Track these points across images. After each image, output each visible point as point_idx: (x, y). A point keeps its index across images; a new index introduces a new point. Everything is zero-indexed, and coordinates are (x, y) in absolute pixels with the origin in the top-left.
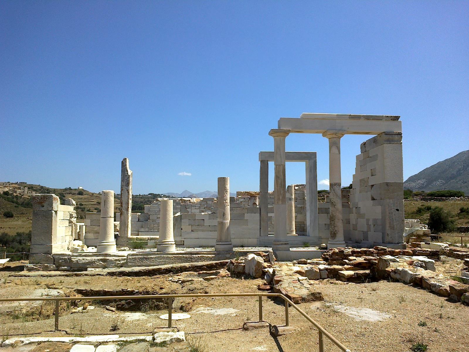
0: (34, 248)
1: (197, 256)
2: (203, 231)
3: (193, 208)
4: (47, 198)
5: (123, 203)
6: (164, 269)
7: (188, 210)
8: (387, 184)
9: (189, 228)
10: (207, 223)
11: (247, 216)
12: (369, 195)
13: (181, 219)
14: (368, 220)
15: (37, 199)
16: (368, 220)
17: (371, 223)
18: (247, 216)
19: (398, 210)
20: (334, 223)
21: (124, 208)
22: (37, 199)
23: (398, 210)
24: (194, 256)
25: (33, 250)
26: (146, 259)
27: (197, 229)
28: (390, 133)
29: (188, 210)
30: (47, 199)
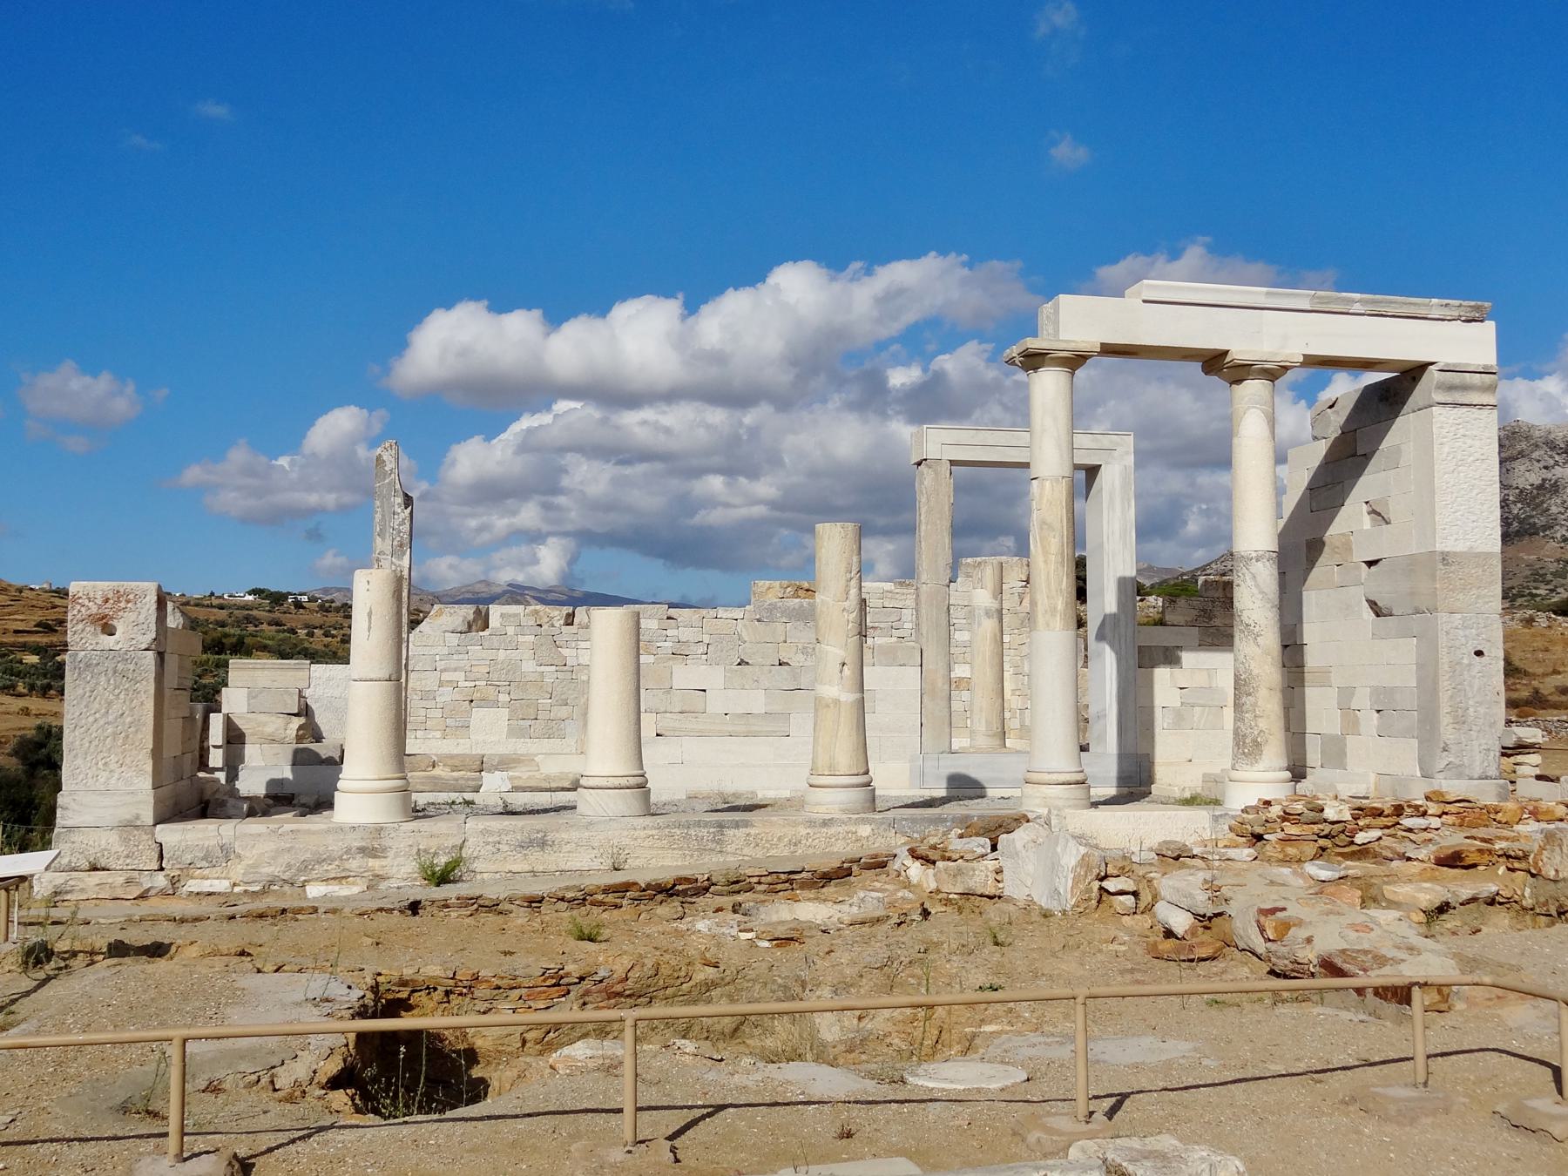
0: (73, 805)
2: (701, 734)
6: (649, 887)
7: (565, 652)
8: (1445, 558)
12: (1358, 596)
14: (1347, 693)
16: (1347, 693)
17: (1363, 700)
19: (1479, 653)
20: (1255, 705)
23: (1479, 653)
25: (69, 813)
26: (543, 844)
27: (677, 725)
29: (565, 652)
30: (128, 601)
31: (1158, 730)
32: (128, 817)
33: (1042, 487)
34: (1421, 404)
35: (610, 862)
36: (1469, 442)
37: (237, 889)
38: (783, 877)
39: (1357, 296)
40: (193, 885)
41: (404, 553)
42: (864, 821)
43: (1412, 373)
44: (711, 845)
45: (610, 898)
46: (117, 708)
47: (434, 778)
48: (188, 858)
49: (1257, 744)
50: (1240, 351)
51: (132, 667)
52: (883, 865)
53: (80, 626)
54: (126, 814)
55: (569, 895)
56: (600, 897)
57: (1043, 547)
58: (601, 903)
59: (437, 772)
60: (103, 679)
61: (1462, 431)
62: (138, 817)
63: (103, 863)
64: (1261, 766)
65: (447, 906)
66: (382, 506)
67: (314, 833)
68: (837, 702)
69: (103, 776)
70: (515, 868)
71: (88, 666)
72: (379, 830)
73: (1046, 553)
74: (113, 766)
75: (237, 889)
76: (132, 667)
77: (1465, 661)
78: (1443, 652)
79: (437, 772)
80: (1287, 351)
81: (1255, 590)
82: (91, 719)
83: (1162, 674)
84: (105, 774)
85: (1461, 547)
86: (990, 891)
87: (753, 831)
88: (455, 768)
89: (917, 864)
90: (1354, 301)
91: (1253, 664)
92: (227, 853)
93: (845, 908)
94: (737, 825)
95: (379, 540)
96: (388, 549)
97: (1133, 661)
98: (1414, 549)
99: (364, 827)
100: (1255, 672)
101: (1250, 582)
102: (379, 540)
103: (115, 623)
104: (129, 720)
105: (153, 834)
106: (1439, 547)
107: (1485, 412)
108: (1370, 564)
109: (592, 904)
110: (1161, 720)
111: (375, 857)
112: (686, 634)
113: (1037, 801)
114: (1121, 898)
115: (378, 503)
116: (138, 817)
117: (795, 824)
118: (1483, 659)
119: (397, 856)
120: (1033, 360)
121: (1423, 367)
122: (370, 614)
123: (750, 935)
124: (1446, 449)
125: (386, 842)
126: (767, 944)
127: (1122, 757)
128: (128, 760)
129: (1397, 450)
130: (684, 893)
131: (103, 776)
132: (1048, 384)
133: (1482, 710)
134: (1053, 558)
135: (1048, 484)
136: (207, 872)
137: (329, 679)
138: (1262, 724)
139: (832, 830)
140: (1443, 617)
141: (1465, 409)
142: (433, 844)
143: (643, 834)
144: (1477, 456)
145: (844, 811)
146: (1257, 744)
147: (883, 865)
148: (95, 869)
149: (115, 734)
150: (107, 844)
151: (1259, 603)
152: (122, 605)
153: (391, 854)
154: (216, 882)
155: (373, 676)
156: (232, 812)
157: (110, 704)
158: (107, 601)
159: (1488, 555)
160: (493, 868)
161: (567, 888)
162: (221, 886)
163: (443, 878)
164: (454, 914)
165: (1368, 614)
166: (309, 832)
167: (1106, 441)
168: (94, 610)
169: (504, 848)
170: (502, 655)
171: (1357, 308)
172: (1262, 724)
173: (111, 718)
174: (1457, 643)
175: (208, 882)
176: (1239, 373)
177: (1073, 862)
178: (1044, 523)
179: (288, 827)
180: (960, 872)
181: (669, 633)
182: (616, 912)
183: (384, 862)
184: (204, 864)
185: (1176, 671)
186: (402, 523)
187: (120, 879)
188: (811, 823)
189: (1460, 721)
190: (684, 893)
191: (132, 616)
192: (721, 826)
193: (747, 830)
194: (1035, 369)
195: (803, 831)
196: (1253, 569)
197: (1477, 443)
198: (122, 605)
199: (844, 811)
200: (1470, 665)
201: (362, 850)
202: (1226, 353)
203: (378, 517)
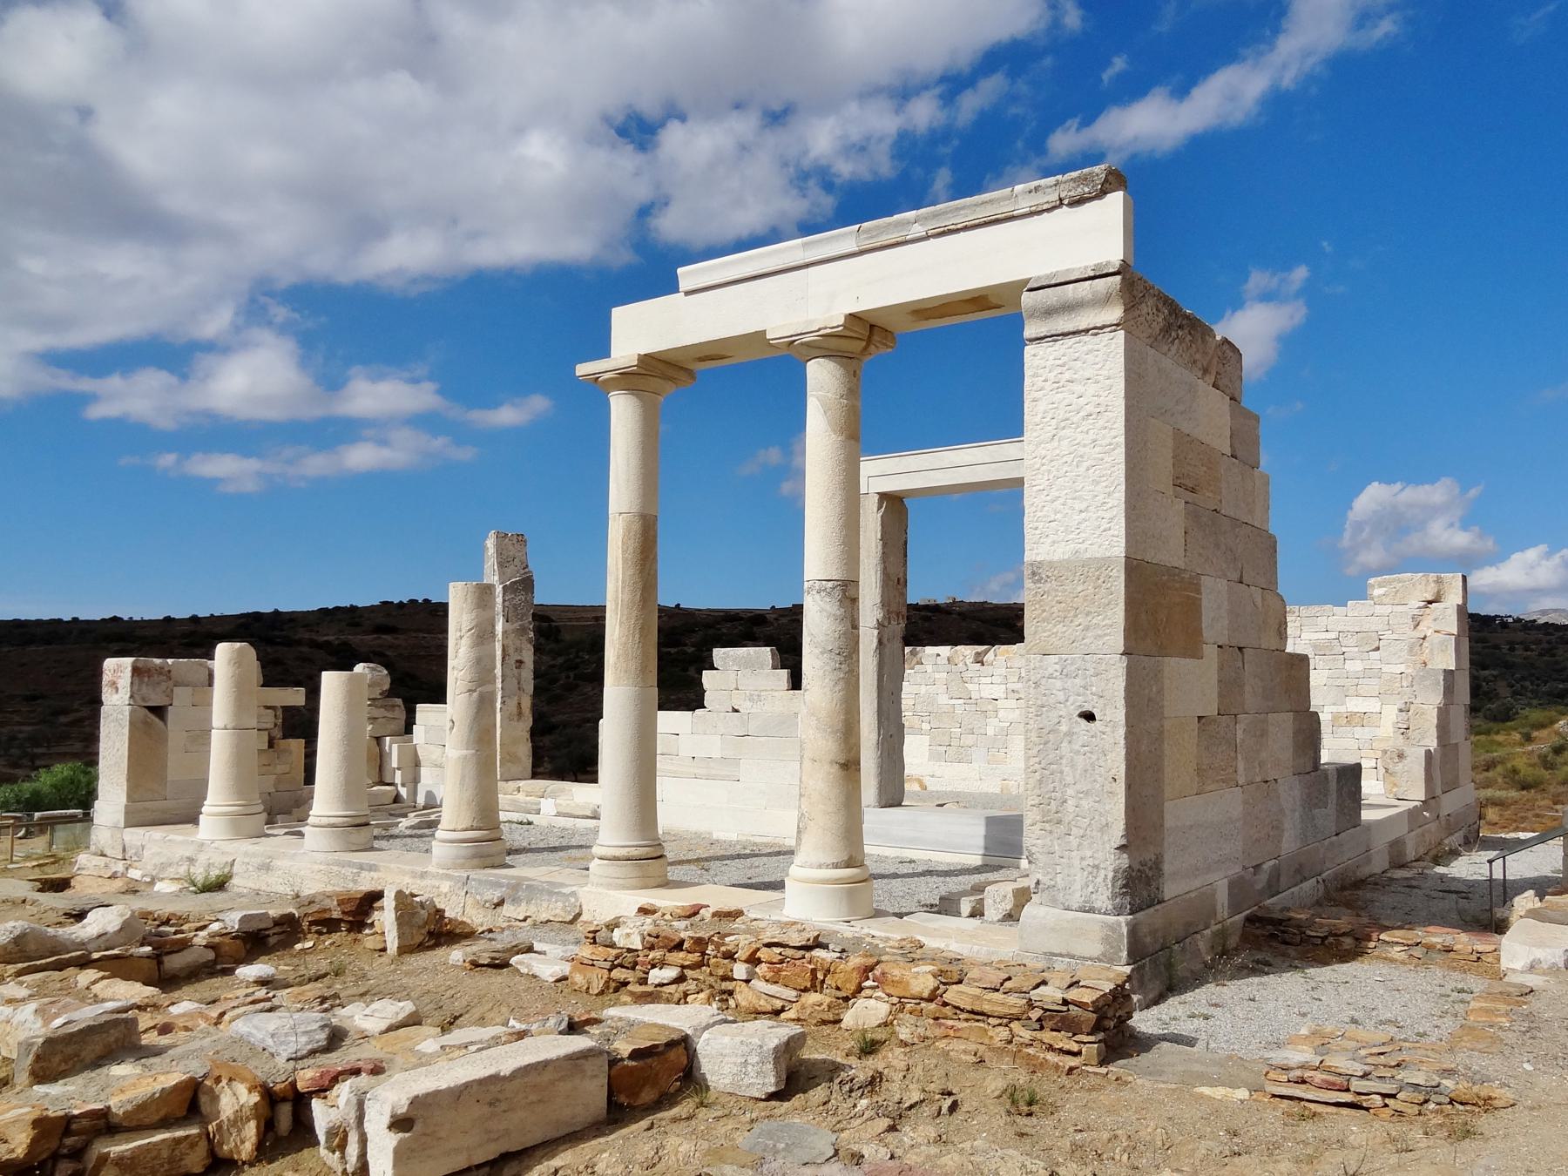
3: (983, 680)
7: (970, 686)
19: (1089, 717)
23: (1089, 717)
28: (1047, 277)
29: (970, 686)
36: (1078, 388)
61: (1067, 376)
77: (1064, 728)
85: (1061, 552)
107: (1105, 337)
118: (1092, 725)
133: (1086, 804)
144: (1090, 408)
159: (1105, 562)
170: (923, 689)
174: (1052, 700)
197: (1092, 389)
200: (1070, 734)
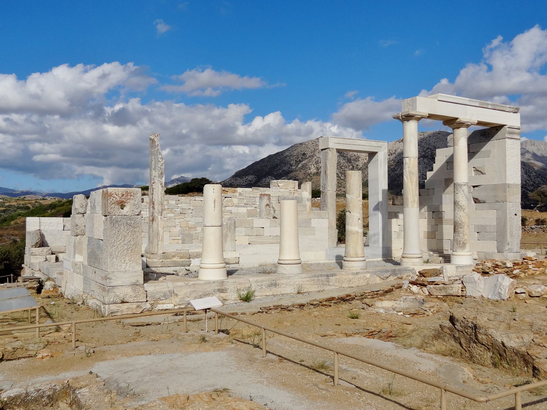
1: (334, 278)
2: (263, 243)
4: (132, 194)
5: (156, 203)
6: (339, 298)
8: (509, 184)
9: (246, 240)
10: (268, 232)
11: (315, 222)
13: (235, 227)
15: (115, 196)
18: (315, 222)
20: (464, 231)
21: (156, 210)
22: (115, 196)
23: (516, 215)
24: (331, 278)
25: (112, 281)
26: (275, 285)
27: (255, 240)
30: (131, 196)
31: (393, 239)
32: (134, 281)
33: (410, 161)
34: (500, 138)
35: (296, 290)
37: (176, 307)
38: (375, 293)
39: (490, 103)
40: (160, 307)
41: (163, 177)
42: (368, 272)
43: (498, 128)
44: (326, 283)
45: (327, 303)
46: (128, 238)
47: (174, 261)
48: (158, 296)
49: (464, 243)
50: (462, 118)
51: (133, 222)
52: (401, 287)
53: (113, 206)
54: (133, 280)
55: (315, 303)
56: (325, 303)
57: (411, 180)
58: (325, 305)
59: (174, 259)
60: (122, 227)
62: (138, 281)
63: (126, 300)
64: (466, 250)
65: (271, 309)
66: (155, 158)
67: (200, 284)
68: (357, 232)
69: (124, 266)
70: (268, 294)
71: (117, 221)
72: (222, 282)
73: (412, 182)
74: (126, 262)
75: (176, 307)
76: (133, 222)
78: (508, 214)
79: (174, 259)
80: (473, 119)
81: (463, 195)
82: (118, 243)
83: (394, 221)
84: (124, 265)
85: (512, 182)
86: (460, 294)
87: (337, 277)
88: (181, 258)
89: (415, 286)
90: (488, 104)
91: (463, 218)
92: (172, 293)
93: (398, 302)
94: (332, 275)
95: (154, 171)
96: (157, 175)
97: (387, 217)
98: (496, 182)
99: (217, 281)
100: (464, 221)
101: (462, 192)
102: (154, 171)
103: (126, 204)
104: (132, 243)
105: (144, 288)
106: (507, 182)
108: (474, 187)
109: (322, 305)
110: (394, 236)
111: (223, 292)
112: (184, 206)
113: (410, 264)
114: (522, 294)
115: (153, 157)
116: (138, 281)
117: (349, 274)
119: (231, 291)
120: (408, 117)
121: (502, 126)
122: (215, 201)
123: (402, 313)
124: (509, 152)
125: (226, 287)
126: (409, 316)
127: (383, 248)
128: (133, 259)
129: (489, 152)
130: (349, 300)
131: (124, 266)
132: (411, 127)
134: (414, 184)
135: (412, 159)
136: (164, 301)
137: (50, 223)
138: (466, 237)
139: (359, 276)
140: (508, 203)
141: (513, 140)
142: (242, 287)
143: (305, 280)
145: (362, 269)
146: (464, 244)
147: (401, 287)
148: (123, 302)
149: (128, 249)
150: (126, 292)
151: (465, 199)
152: (129, 197)
153: (229, 291)
154: (168, 305)
155: (216, 225)
156: (151, 277)
157: (125, 237)
158: (123, 195)
160: (261, 294)
161: (314, 300)
162: (170, 306)
163: (247, 299)
164: (273, 312)
165: (473, 202)
166: (199, 284)
167: (380, 144)
168: (118, 199)
169: (264, 287)
171: (490, 107)
172: (466, 237)
173: (126, 242)
175: (165, 305)
176: (462, 124)
177: (508, 284)
178: (411, 172)
179: (191, 283)
180: (444, 288)
181: (179, 205)
182: (330, 308)
183: (227, 294)
184: (163, 298)
185: (398, 220)
186: (162, 165)
187: (135, 306)
188: (353, 274)
189: (511, 235)
190: (349, 300)
191: (133, 202)
192: (328, 276)
193: (336, 277)
194: (408, 121)
195: (352, 277)
196: (463, 188)
198: (129, 197)
199: (362, 269)
201: (219, 290)
202: (457, 119)
203: (153, 162)
